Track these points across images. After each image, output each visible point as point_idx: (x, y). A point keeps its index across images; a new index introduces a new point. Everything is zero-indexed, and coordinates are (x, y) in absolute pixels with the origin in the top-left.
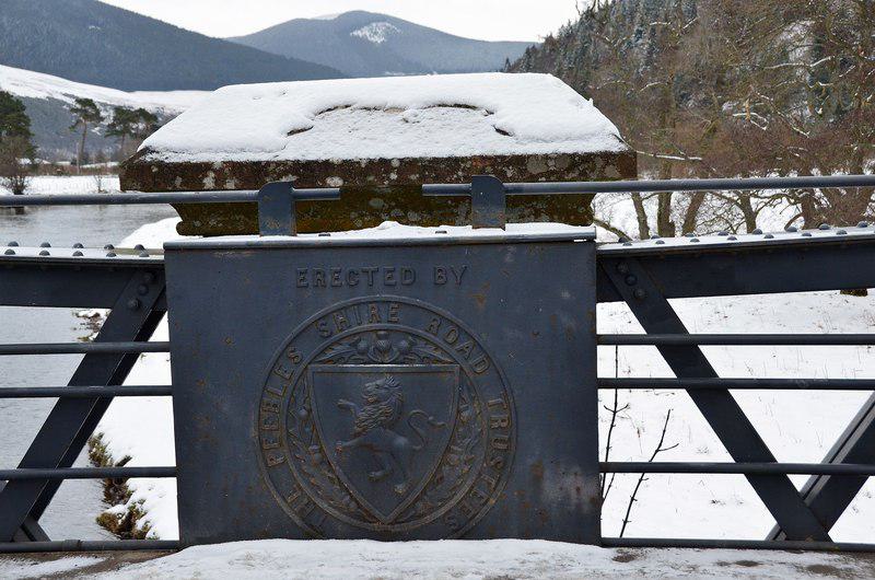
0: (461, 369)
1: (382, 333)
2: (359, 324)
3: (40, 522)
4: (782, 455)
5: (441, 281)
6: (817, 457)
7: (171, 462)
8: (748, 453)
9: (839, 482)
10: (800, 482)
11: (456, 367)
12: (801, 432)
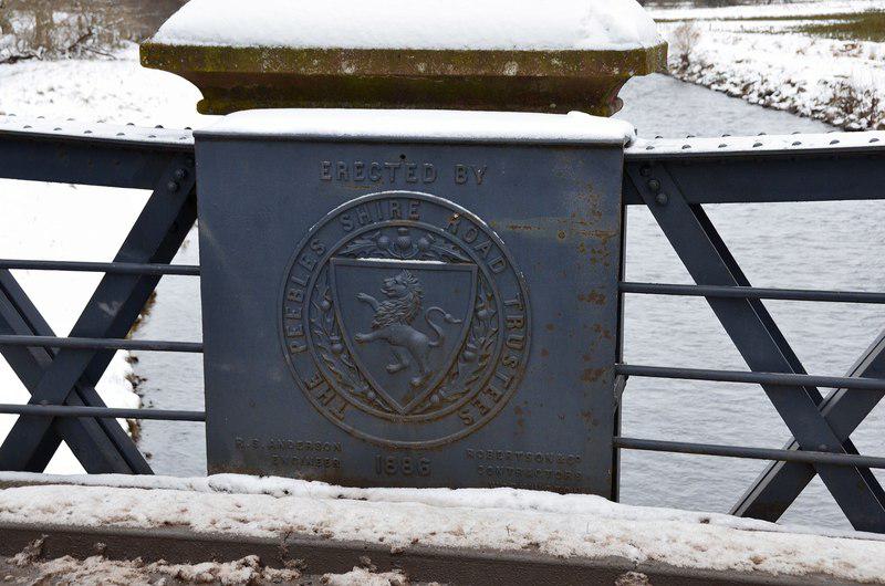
0: (479, 268)
1: (403, 229)
2: (381, 220)
3: (98, 388)
4: (813, 369)
5: (462, 180)
6: (840, 372)
7: (198, 339)
8: (769, 358)
9: (858, 398)
10: (825, 392)
11: (474, 267)
12: (827, 345)
